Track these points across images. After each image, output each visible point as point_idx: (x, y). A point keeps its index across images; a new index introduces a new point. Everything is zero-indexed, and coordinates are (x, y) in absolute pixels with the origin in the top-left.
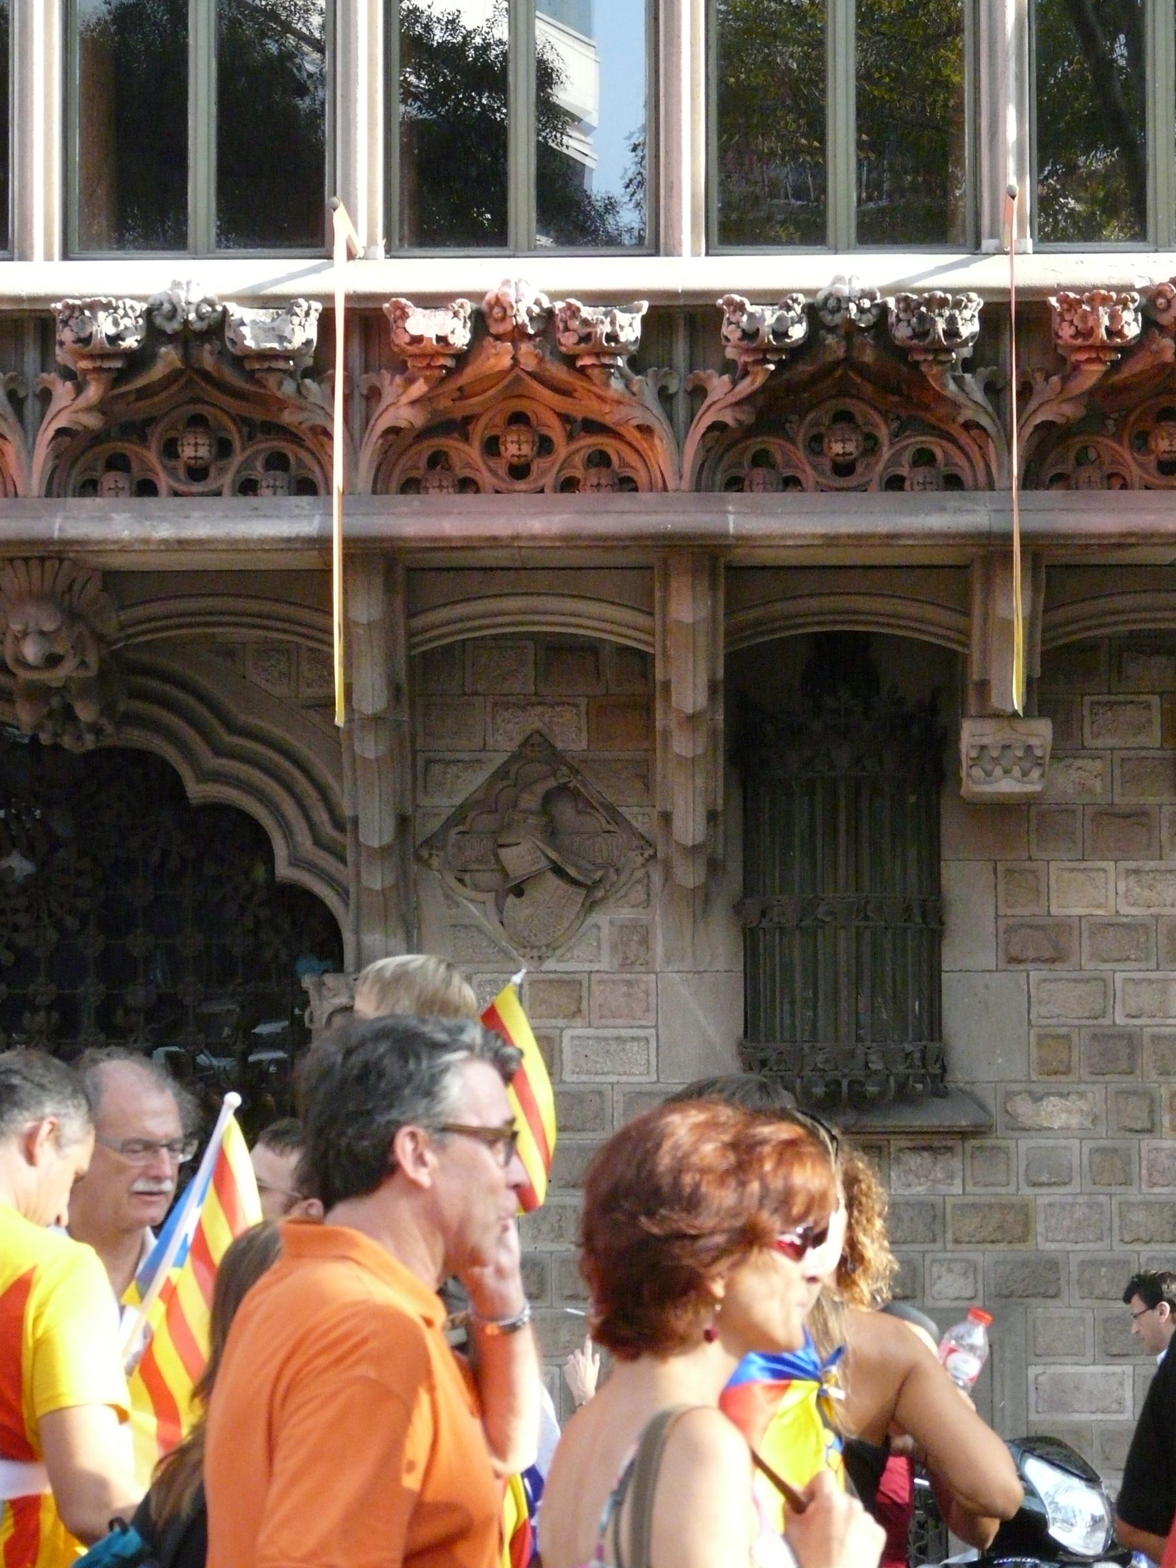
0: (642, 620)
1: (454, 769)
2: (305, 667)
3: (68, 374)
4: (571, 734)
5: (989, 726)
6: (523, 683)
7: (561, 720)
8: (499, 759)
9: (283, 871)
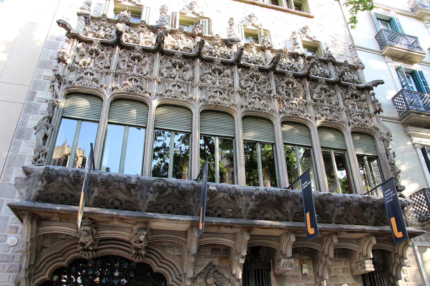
0: (234, 242)
1: (199, 267)
2: (176, 250)
3: (151, 192)
4: (216, 262)
5: (286, 259)
6: (209, 254)
8: (205, 266)
9: (171, 282)
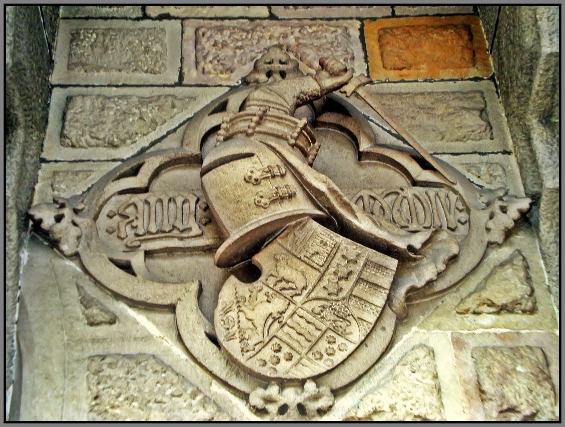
7: (316, 42)
